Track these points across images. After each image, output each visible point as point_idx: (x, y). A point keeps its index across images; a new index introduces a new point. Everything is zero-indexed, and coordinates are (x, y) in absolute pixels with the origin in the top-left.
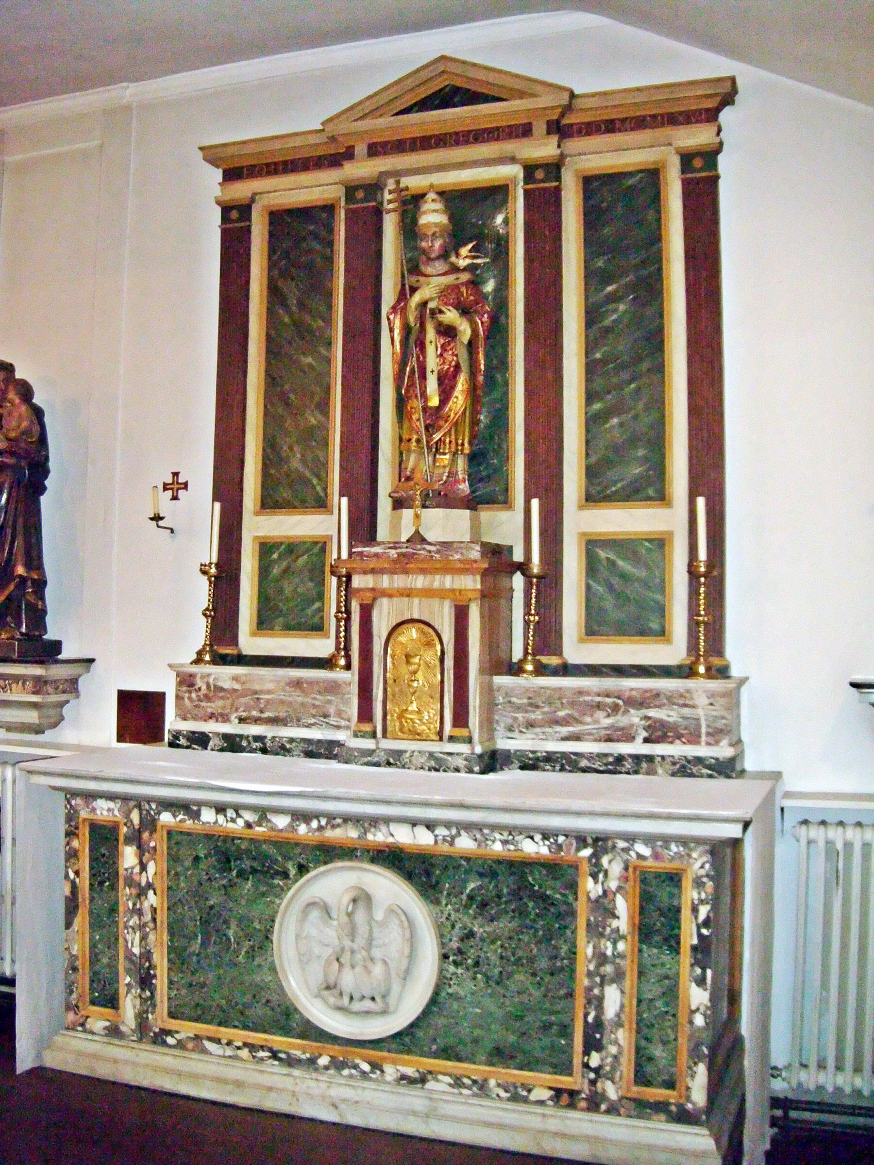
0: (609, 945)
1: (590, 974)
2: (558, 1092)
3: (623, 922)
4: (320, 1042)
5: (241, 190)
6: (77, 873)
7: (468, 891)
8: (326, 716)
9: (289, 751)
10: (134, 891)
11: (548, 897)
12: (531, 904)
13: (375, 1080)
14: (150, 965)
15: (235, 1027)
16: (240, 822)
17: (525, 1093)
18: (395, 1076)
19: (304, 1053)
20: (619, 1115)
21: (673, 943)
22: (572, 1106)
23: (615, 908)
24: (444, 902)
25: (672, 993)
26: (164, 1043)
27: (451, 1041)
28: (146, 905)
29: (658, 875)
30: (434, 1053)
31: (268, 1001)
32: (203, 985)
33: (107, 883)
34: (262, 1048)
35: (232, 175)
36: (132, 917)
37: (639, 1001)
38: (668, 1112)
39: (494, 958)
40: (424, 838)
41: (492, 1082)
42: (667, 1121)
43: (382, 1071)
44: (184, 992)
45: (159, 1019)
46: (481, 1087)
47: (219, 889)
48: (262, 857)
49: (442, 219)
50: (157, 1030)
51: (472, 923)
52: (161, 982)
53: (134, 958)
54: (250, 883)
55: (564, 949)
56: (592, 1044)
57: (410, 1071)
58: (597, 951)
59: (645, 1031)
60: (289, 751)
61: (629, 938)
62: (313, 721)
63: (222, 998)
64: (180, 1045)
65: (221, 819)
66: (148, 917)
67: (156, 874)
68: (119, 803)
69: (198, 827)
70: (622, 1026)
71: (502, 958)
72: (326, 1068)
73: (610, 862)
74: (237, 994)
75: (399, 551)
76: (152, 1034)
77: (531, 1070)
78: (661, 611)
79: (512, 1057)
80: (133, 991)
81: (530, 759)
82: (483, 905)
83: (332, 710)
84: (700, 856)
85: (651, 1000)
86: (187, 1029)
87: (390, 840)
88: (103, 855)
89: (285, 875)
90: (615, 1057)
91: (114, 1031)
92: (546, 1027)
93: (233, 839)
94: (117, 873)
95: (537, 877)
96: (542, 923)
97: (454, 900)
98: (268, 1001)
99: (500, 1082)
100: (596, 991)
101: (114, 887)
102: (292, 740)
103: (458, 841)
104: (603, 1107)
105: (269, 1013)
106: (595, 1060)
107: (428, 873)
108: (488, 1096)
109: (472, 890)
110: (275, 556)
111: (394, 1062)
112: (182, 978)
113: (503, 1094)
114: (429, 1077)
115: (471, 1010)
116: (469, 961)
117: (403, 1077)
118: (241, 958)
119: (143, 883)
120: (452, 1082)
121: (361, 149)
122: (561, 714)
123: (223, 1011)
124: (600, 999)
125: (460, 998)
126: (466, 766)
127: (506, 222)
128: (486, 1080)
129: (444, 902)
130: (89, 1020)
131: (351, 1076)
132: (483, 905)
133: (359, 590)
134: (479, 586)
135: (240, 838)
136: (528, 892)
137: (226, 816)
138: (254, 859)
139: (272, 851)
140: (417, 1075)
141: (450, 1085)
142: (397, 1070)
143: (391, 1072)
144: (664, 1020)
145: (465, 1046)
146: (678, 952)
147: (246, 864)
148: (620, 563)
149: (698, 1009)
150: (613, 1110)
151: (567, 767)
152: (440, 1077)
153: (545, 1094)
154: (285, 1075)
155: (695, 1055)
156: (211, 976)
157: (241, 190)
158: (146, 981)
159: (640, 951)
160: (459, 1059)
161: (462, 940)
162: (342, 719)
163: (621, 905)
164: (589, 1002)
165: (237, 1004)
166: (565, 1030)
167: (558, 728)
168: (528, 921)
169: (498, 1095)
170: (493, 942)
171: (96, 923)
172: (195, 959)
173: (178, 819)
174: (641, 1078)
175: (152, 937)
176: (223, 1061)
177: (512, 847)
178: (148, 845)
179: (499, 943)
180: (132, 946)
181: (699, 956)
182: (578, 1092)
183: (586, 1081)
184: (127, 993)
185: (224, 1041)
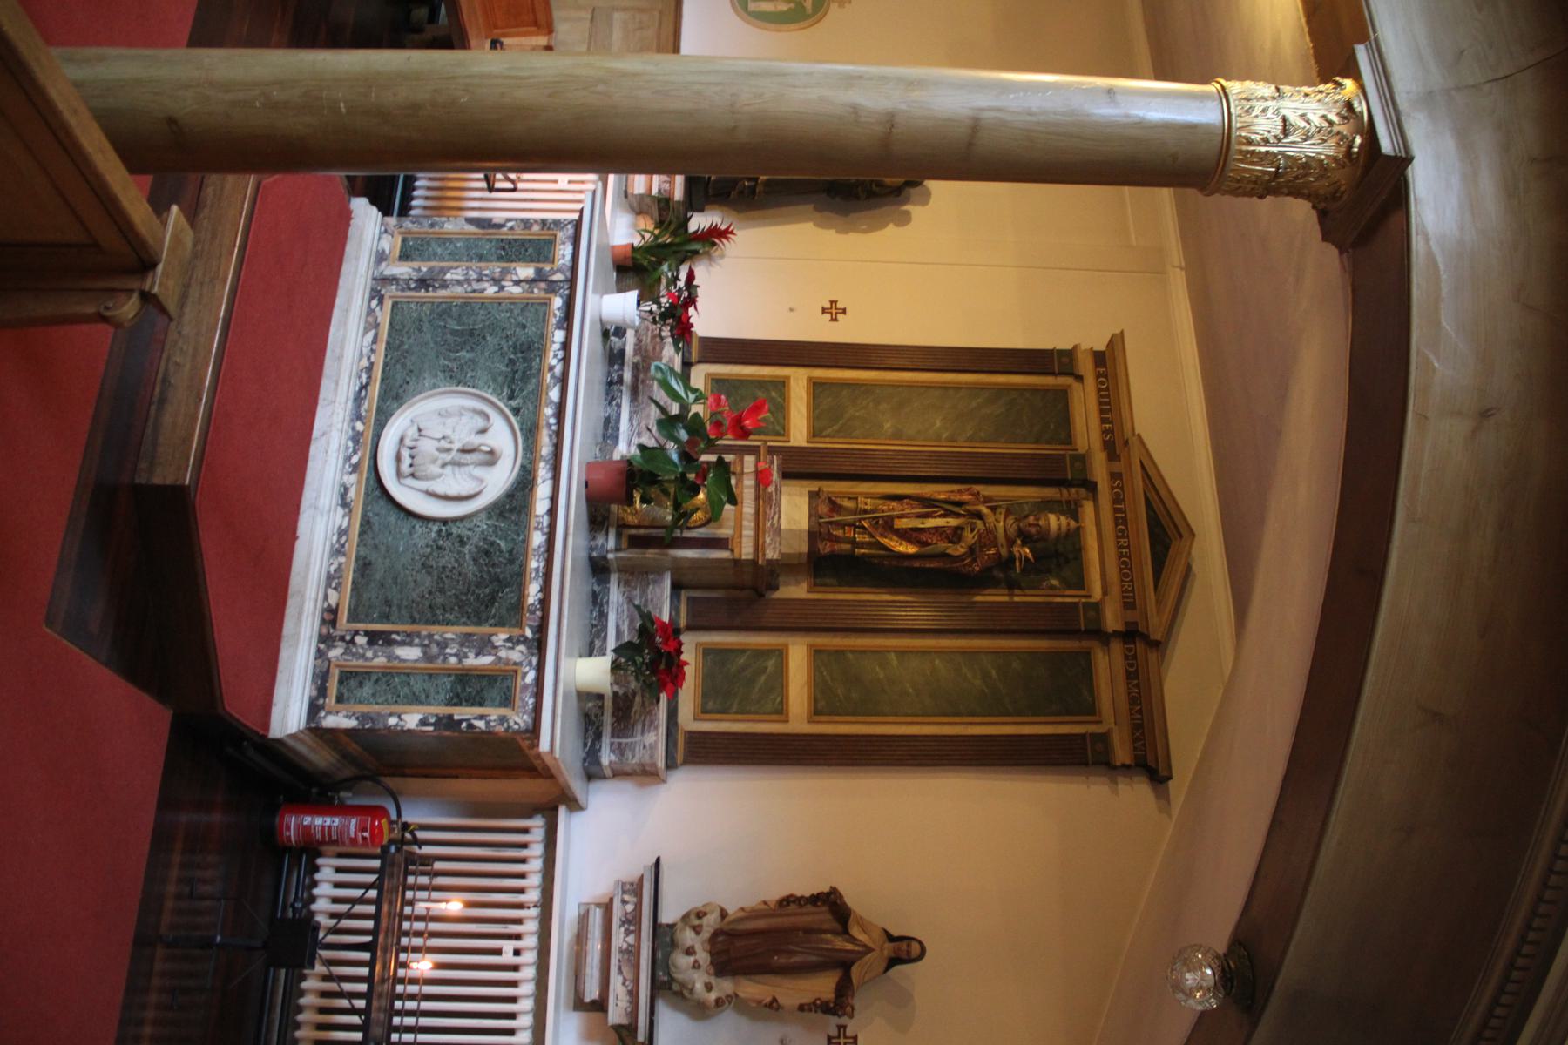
0: (454, 651)
1: (430, 636)
3: (472, 661)
5: (1086, 367)
6: (512, 228)
7: (498, 541)
9: (610, 404)
10: (497, 276)
11: (493, 604)
12: (487, 591)
14: (436, 288)
15: (386, 356)
16: (554, 362)
17: (334, 585)
18: (347, 483)
19: (366, 411)
20: (316, 659)
21: (455, 701)
22: (323, 622)
23: (484, 655)
24: (489, 522)
25: (415, 700)
26: (372, 298)
27: (376, 528)
28: (486, 285)
29: (508, 688)
30: (366, 515)
32: (420, 330)
33: (503, 254)
34: (369, 377)
35: (1100, 358)
36: (476, 273)
37: (408, 675)
38: (317, 698)
39: (443, 562)
40: (541, 506)
41: (342, 559)
42: (310, 697)
43: (351, 473)
44: (415, 315)
46: (338, 551)
47: (499, 345)
48: (525, 378)
50: (383, 292)
51: (471, 545)
54: (504, 369)
56: (373, 637)
57: (351, 494)
58: (450, 642)
59: (384, 679)
60: (610, 404)
61: (460, 666)
62: (635, 423)
63: (409, 346)
64: (371, 312)
65: (557, 346)
66: (476, 286)
69: (550, 328)
70: (389, 661)
71: (444, 567)
72: (353, 429)
73: (521, 652)
74: (413, 358)
75: (774, 494)
76: (379, 288)
77: (352, 590)
79: (362, 576)
80: (415, 274)
81: (602, 600)
82: (487, 553)
84: (524, 721)
85: (409, 684)
86: (384, 317)
87: (540, 481)
88: (526, 250)
89: (511, 397)
90: (363, 656)
91: (381, 257)
92: (388, 603)
93: (540, 356)
94: (512, 261)
95: (509, 596)
96: (472, 598)
97: (491, 530)
98: (408, 383)
99: (343, 566)
100: (417, 641)
101: (500, 258)
102: (619, 406)
103: (539, 533)
104: (322, 646)
105: (398, 384)
106: (361, 640)
107: (512, 510)
109: (499, 545)
110: (773, 394)
111: (359, 482)
112: (426, 314)
113: (332, 569)
114: (347, 510)
115: (402, 543)
116: (441, 542)
117: (346, 490)
118: (442, 361)
119: (504, 283)
120: (343, 527)
123: (399, 346)
124: (410, 644)
126: (597, 546)
127: (1052, 587)
128: (344, 554)
129: (489, 522)
130: (390, 237)
131: (347, 448)
132: (487, 553)
133: (742, 461)
134: (743, 557)
135: (541, 361)
136: (497, 588)
138: (524, 372)
139: (531, 387)
140: (348, 500)
141: (340, 527)
143: (351, 479)
144: (393, 694)
146: (447, 705)
147: (520, 366)
148: (763, 678)
149: (401, 719)
150: (320, 654)
151: (594, 630)
152: (347, 519)
153: (333, 598)
154: (348, 396)
155: (363, 718)
156: (429, 336)
160: (361, 534)
161: (459, 536)
163: (486, 660)
165: (405, 358)
166: (385, 618)
167: (626, 623)
168: (473, 588)
169: (332, 564)
170: (457, 561)
171: (470, 242)
172: (442, 324)
174: (346, 676)
175: (459, 290)
176: (358, 346)
177: (533, 575)
178: (534, 288)
179: (456, 565)
181: (444, 721)
183: (343, 633)
185: (374, 347)
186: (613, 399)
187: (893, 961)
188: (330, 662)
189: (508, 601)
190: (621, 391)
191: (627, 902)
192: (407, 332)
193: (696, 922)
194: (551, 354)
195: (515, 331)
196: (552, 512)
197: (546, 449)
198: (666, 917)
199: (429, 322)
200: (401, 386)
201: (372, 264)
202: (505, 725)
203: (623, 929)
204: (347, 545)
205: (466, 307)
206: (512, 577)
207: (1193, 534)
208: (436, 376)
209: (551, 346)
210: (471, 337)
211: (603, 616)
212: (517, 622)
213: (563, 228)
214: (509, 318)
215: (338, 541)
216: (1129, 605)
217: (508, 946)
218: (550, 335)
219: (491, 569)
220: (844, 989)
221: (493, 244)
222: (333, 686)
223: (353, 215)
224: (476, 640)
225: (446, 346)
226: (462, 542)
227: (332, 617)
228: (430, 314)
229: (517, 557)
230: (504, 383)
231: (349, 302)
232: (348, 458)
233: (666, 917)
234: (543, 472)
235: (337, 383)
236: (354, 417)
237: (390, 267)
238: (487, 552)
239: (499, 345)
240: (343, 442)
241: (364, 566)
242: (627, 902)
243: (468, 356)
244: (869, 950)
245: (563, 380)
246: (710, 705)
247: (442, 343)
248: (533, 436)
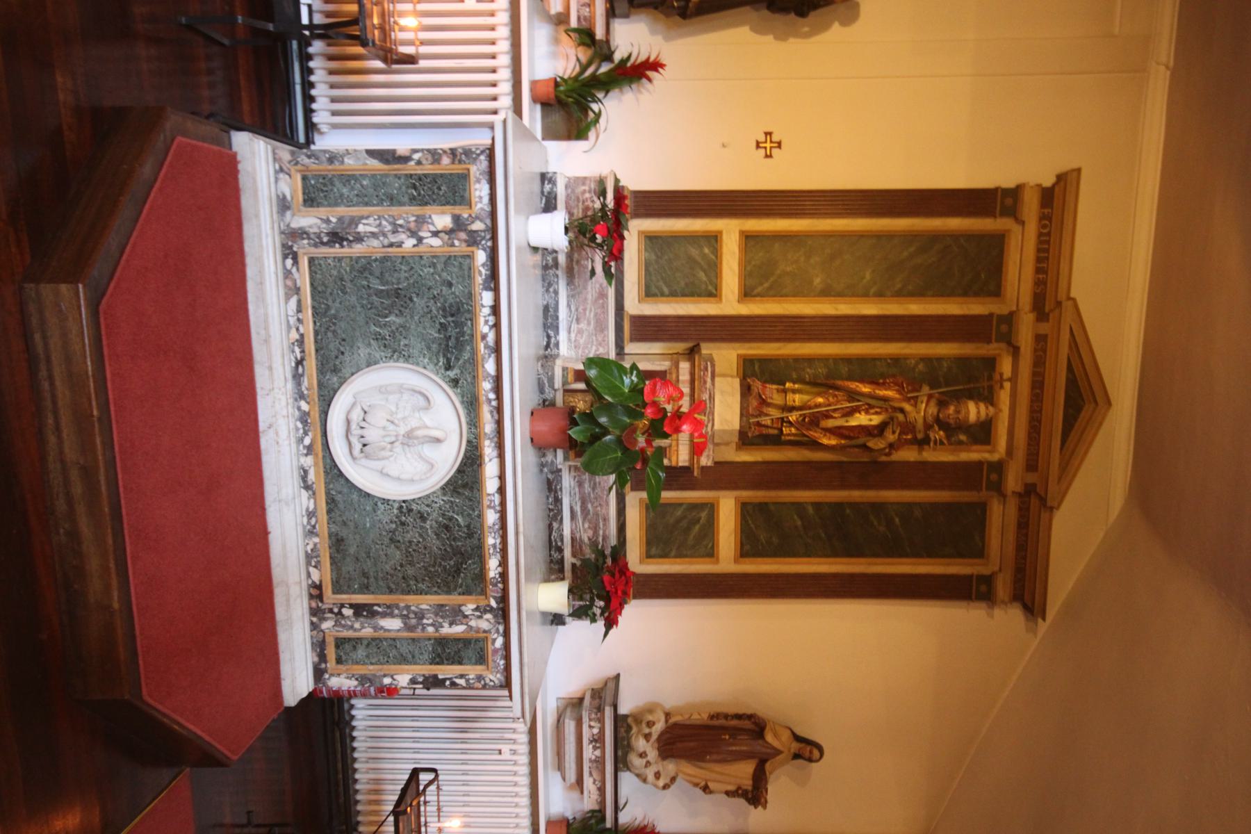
0: (430, 621)
1: (408, 607)
2: (318, 587)
3: (447, 630)
4: (319, 400)
6: (419, 163)
7: (456, 516)
8: (578, 321)
9: (547, 291)
10: (412, 225)
11: (459, 575)
12: (452, 563)
13: (298, 450)
14: (351, 241)
15: (315, 323)
16: (485, 329)
17: (313, 564)
18: (305, 465)
19: (307, 389)
20: (311, 631)
21: (437, 660)
22: (311, 597)
23: (457, 625)
24: (445, 498)
25: (403, 660)
26: (285, 257)
27: (341, 506)
28: (402, 237)
29: (482, 649)
30: (329, 493)
31: (343, 353)
32: (345, 293)
33: (415, 194)
34: (303, 352)
35: (1047, 196)
36: (390, 223)
37: (394, 639)
38: (320, 663)
40: (491, 485)
41: (316, 540)
42: (313, 663)
43: (306, 455)
44: (335, 273)
45: (304, 249)
46: (311, 532)
47: (428, 307)
48: (460, 346)
49: (973, 417)
50: (295, 249)
51: (432, 520)
52: (336, 250)
53: (353, 226)
54: (436, 335)
55: (422, 586)
57: (311, 477)
58: (426, 612)
59: (374, 644)
60: (547, 291)
61: (437, 634)
62: (573, 309)
63: (337, 311)
64: (287, 274)
65: (486, 311)
66: (393, 239)
67: (432, 246)
68: (488, 209)
69: (477, 289)
70: (375, 631)
72: (299, 408)
73: (487, 620)
74: (343, 325)
75: (708, 402)
77: (331, 564)
78: (664, 555)
79: (338, 551)
80: (324, 225)
81: (556, 487)
82: (447, 527)
83: (583, 325)
84: (498, 679)
85: (396, 647)
86: (303, 278)
87: (487, 459)
88: (439, 189)
89: (448, 367)
90: (352, 627)
91: (283, 205)
92: (365, 575)
94: (426, 204)
95: (473, 567)
96: (439, 570)
97: (448, 506)
98: (343, 353)
99: (318, 546)
100: (396, 612)
101: (413, 200)
102: (556, 293)
103: (492, 511)
104: (315, 619)
105: (333, 354)
106: (348, 612)
107: (465, 486)
108: (305, 536)
109: (457, 520)
110: (706, 251)
111: (316, 464)
112: (345, 270)
113: (309, 548)
114: (310, 492)
115: (368, 520)
116: (404, 518)
117: (306, 472)
118: (373, 328)
119: (422, 234)
120: (311, 510)
121: (1044, 328)
122: (590, 506)
123: (326, 312)
124: (392, 615)
125: (375, 512)
126: (547, 462)
127: (960, 443)
128: (317, 535)
129: (445, 498)
130: (287, 177)
131: (297, 429)
132: (447, 527)
133: (677, 367)
134: (680, 464)
135: (472, 325)
137: (489, 315)
138: (457, 339)
139: (466, 356)
140: (310, 483)
141: (307, 509)
142: (310, 467)
143: (308, 461)
144: (384, 655)
145: (340, 516)
146: (431, 664)
147: (452, 332)
148: (697, 527)
149: (394, 680)
150: (314, 626)
151: (551, 514)
152: (312, 501)
156: (354, 299)
157: (1031, 207)
158: (336, 237)
159: (430, 639)
160: (329, 511)
161: (419, 512)
162: (576, 335)
164: (388, 607)
165: (334, 324)
166: (365, 589)
167: (579, 504)
168: (439, 560)
169: (308, 544)
170: (421, 535)
171: (378, 181)
172: (365, 283)
173: (481, 269)
174: (340, 643)
175: (375, 243)
176: (283, 317)
177: (491, 551)
178: (453, 239)
179: (421, 540)
180: (364, 224)
181: (431, 680)
182: (322, 601)
183: (331, 606)
184: (321, 219)
186: (550, 285)
187: (797, 756)
188: (324, 633)
189: (472, 572)
190: (557, 276)
191: (593, 727)
192: (331, 294)
193: (647, 731)
194: (482, 320)
195: (441, 290)
196: (502, 490)
197: (488, 427)
198: (623, 709)
199: (351, 281)
200: (337, 357)
201: (275, 216)
202: (483, 682)
203: (591, 746)
204: (317, 526)
206: (472, 549)
207: (1109, 403)
208: (369, 345)
209: (480, 311)
210: (399, 298)
211: (558, 501)
212: (482, 591)
213: (475, 159)
214: (433, 274)
215: (309, 523)
216: (1032, 465)
217: (505, 748)
218: (478, 297)
219: (453, 543)
220: (760, 779)
221: (402, 180)
222: (331, 652)
223: (239, 158)
224: (448, 610)
225: (373, 311)
226: (423, 518)
227: (318, 592)
228: (351, 272)
229: (474, 532)
230: (438, 352)
231: (261, 272)
232: (301, 440)
233: (623, 709)
235: (270, 368)
236: (298, 397)
237: (296, 217)
238: (446, 527)
239: (428, 307)
240: (292, 426)
241: (337, 543)
242: (593, 727)
243: (398, 320)
244: (778, 752)
245: (497, 350)
246: (653, 551)
247: (369, 306)
248: (474, 410)
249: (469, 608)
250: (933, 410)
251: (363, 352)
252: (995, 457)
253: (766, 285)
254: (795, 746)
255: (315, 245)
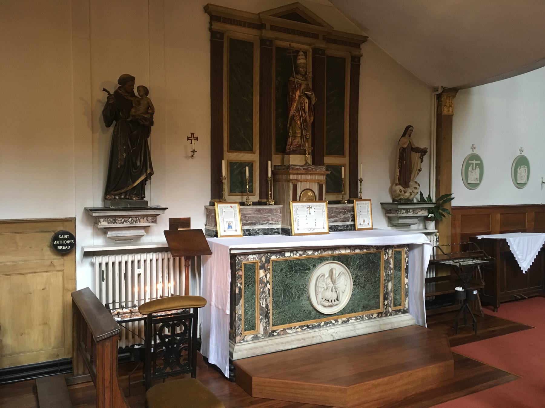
2: (378, 314)
3: (392, 266)
4: (320, 318)
5: (217, 26)
6: (241, 284)
8: (268, 220)
10: (263, 285)
11: (374, 262)
12: (371, 264)
13: (336, 325)
14: (268, 310)
15: (294, 322)
16: (298, 255)
17: (372, 316)
20: (392, 315)
21: (400, 268)
22: (381, 316)
24: (351, 268)
25: (400, 281)
26: (273, 336)
28: (266, 289)
31: (304, 310)
34: (305, 326)
36: (262, 294)
37: (394, 285)
39: (363, 281)
41: (364, 316)
42: (401, 314)
43: (338, 322)
45: (270, 328)
46: (362, 318)
47: (289, 278)
50: (270, 332)
51: (358, 273)
52: (271, 315)
53: (263, 309)
57: (345, 319)
62: (264, 223)
64: (279, 334)
65: (292, 254)
66: (267, 293)
67: (270, 277)
68: (258, 255)
69: (284, 259)
70: (392, 292)
71: (364, 281)
72: (323, 326)
74: (295, 311)
75: (304, 168)
76: (268, 334)
77: (371, 310)
80: (263, 321)
85: (396, 284)
86: (280, 328)
89: (309, 269)
90: (391, 300)
91: (256, 338)
92: (374, 297)
93: (294, 260)
94: (255, 280)
97: (353, 267)
99: (366, 315)
100: (386, 284)
101: (253, 286)
102: (259, 230)
104: (389, 314)
108: (363, 320)
110: (235, 167)
111: (341, 318)
112: (276, 311)
115: (357, 297)
116: (357, 283)
118: (296, 299)
119: (265, 281)
120: (355, 319)
121: (268, 26)
124: (387, 286)
125: (355, 294)
128: (363, 316)
130: (246, 337)
131: (330, 326)
132: (360, 267)
136: (370, 262)
137: (293, 253)
139: (306, 262)
141: (355, 320)
142: (342, 320)
143: (340, 321)
145: (356, 308)
146: (401, 271)
152: (352, 318)
154: (314, 332)
156: (286, 307)
158: (267, 316)
159: (394, 272)
161: (355, 278)
162: (274, 221)
163: (392, 261)
164: (385, 287)
165: (295, 314)
166: (378, 297)
167: (332, 219)
169: (366, 319)
170: (362, 277)
173: (277, 257)
174: (395, 305)
175: (268, 300)
176: (293, 334)
178: (267, 268)
180: (262, 305)
182: (383, 312)
183: (384, 309)
184: (261, 322)
185: (293, 328)
186: (256, 232)
188: (393, 311)
189: (374, 257)
190: (253, 229)
191: (403, 212)
192: (285, 317)
193: (403, 192)
194: (295, 256)
195: (284, 273)
199: (280, 309)
200: (306, 313)
201: (260, 340)
202: (407, 252)
203: (409, 213)
204: (360, 316)
205: (275, 295)
206: (367, 257)
208: (302, 300)
209: (292, 257)
212: (379, 253)
213: (240, 261)
214: (278, 277)
215: (359, 319)
218: (287, 258)
219: (365, 265)
220: (417, 150)
221: (246, 290)
222: (398, 308)
224: (386, 265)
225: (290, 299)
226: (357, 276)
227: (380, 314)
228: (277, 309)
230: (304, 273)
232: (333, 324)
234: (337, 252)
235: (313, 337)
236: (319, 327)
237: (260, 332)
238: (360, 267)
239: (289, 278)
240: (330, 328)
242: (403, 212)
243: (294, 289)
247: (289, 301)
248: (323, 258)
249: (385, 258)
250: (299, 76)
251: (304, 302)
252: (311, 50)
253: (248, 142)
254: (407, 136)
255: (269, 324)
